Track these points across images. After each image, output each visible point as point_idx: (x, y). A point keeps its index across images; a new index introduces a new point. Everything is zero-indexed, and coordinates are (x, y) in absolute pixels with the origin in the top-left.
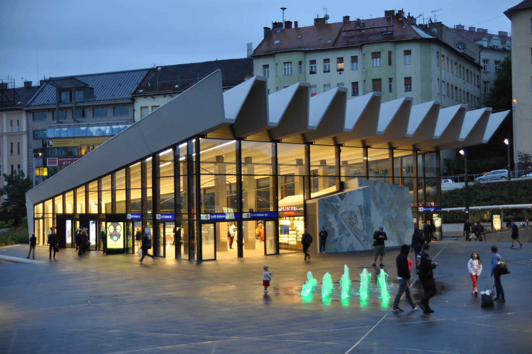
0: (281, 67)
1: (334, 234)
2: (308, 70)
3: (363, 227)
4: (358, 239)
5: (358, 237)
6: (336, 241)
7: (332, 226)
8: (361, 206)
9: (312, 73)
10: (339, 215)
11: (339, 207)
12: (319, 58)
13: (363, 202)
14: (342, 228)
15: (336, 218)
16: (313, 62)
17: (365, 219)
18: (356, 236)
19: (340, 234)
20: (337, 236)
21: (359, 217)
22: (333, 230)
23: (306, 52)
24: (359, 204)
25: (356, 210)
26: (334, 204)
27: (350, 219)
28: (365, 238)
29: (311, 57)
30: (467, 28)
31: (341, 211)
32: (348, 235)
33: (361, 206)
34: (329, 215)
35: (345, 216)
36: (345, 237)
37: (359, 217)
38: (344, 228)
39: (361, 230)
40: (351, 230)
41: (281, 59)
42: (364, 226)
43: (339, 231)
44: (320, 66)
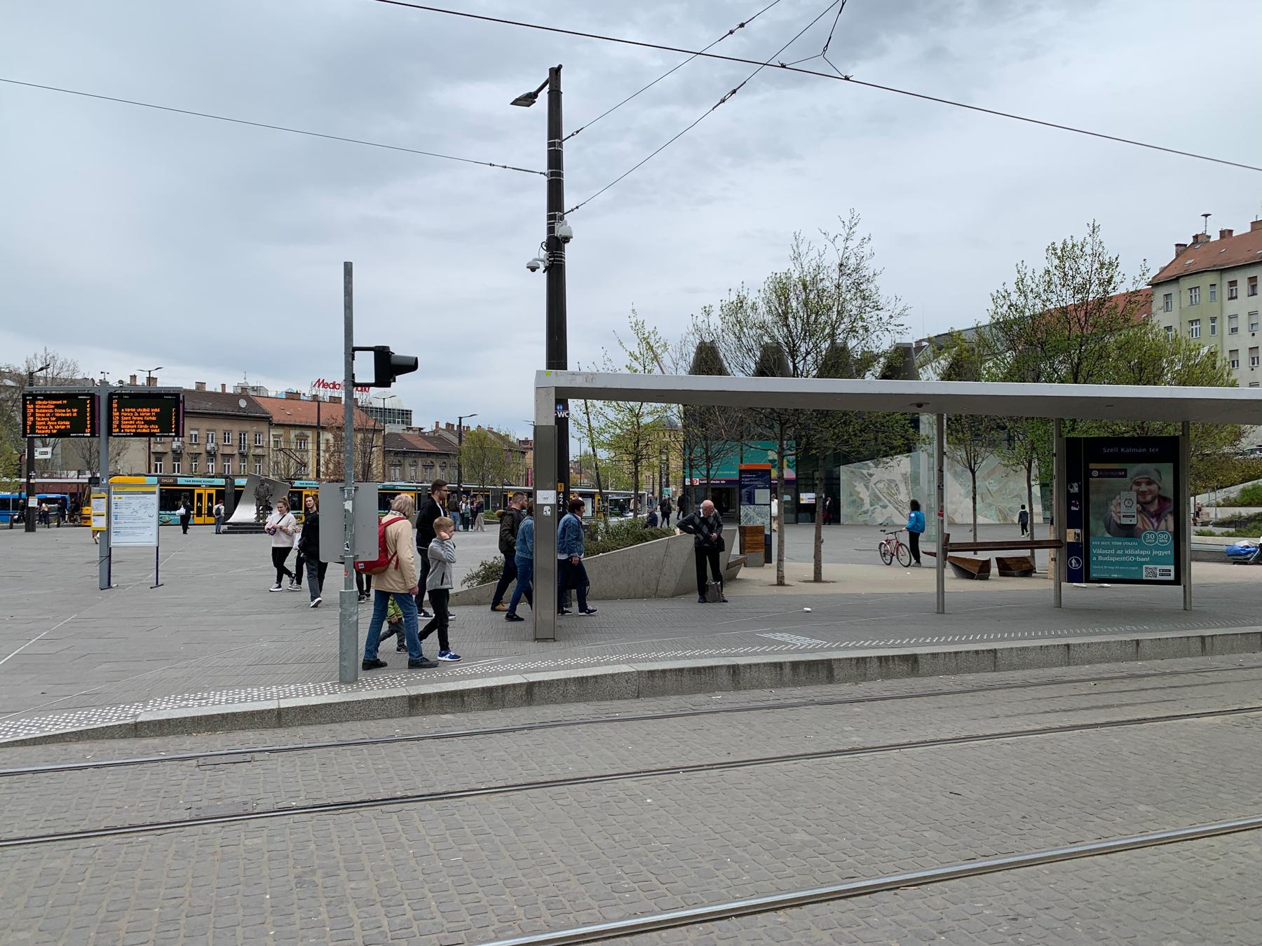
0: (1186, 296)
2: (1226, 296)
6: (866, 512)
9: (1231, 298)
10: (871, 484)
11: (871, 475)
12: (1242, 278)
13: (909, 470)
14: (875, 499)
15: (867, 487)
16: (1233, 283)
20: (867, 506)
21: (902, 488)
23: (1222, 271)
25: (898, 478)
26: (865, 472)
29: (1230, 277)
30: (1189, 241)
31: (874, 480)
35: (880, 485)
37: (902, 488)
38: (880, 499)
41: (1186, 284)
44: (1243, 287)
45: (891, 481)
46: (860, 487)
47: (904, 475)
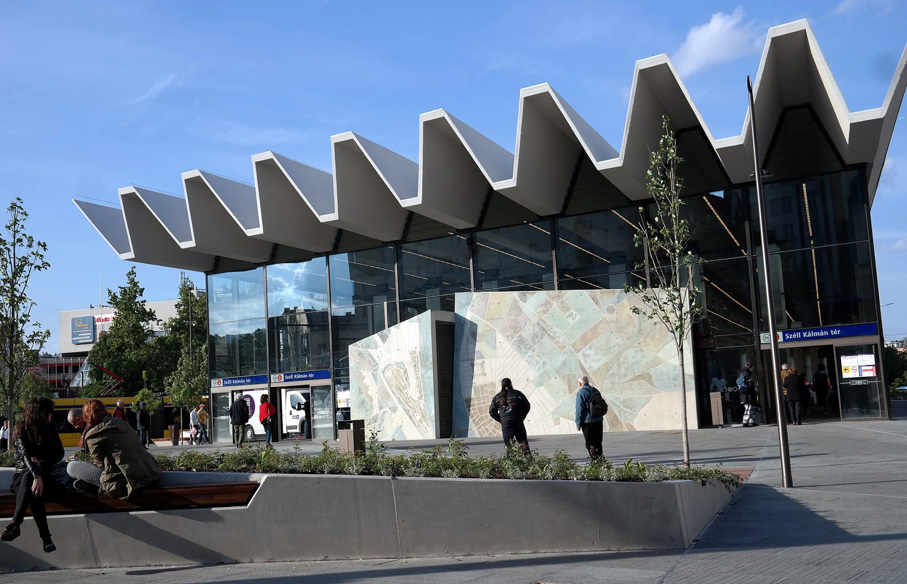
1: (372, 407)
3: (418, 395)
4: (410, 417)
5: (411, 413)
7: (369, 393)
8: (415, 352)
14: (384, 395)
17: (423, 377)
18: (407, 412)
19: (381, 408)
22: (371, 399)
24: (412, 348)
25: (407, 359)
27: (396, 378)
28: (423, 416)
32: (394, 410)
33: (415, 352)
34: (364, 373)
35: (389, 374)
36: (390, 412)
39: (416, 399)
40: (398, 399)
42: (420, 392)
43: (380, 402)
45: (400, 365)
46: (368, 380)
47: (413, 353)
